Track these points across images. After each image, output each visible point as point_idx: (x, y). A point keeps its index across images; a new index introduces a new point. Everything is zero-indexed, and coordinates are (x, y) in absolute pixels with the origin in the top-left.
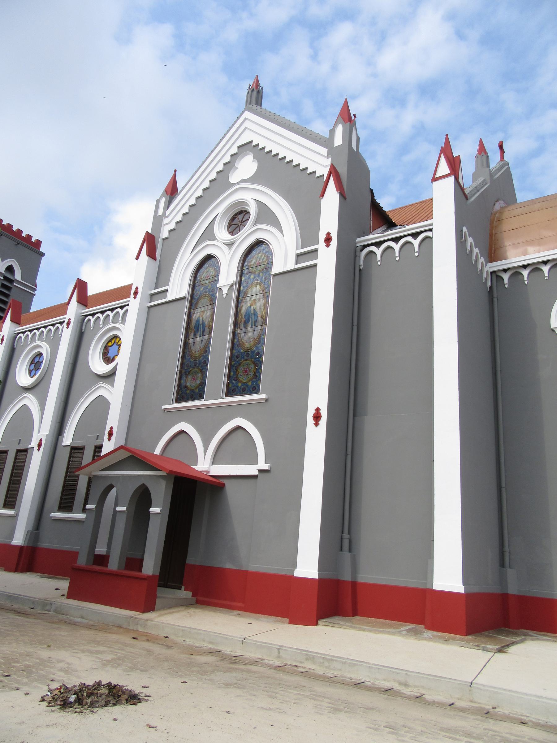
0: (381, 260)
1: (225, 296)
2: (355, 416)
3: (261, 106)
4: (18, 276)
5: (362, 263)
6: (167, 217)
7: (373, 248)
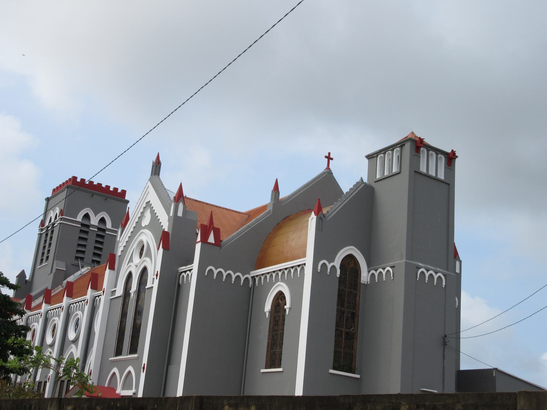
0: (186, 281)
1: (132, 298)
2: (170, 365)
3: (159, 175)
4: (109, 225)
5: (180, 282)
6: (121, 242)
7: (183, 274)
